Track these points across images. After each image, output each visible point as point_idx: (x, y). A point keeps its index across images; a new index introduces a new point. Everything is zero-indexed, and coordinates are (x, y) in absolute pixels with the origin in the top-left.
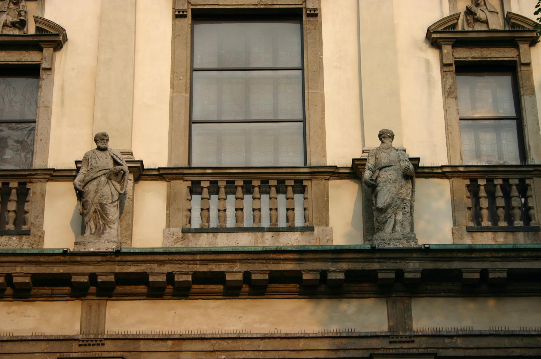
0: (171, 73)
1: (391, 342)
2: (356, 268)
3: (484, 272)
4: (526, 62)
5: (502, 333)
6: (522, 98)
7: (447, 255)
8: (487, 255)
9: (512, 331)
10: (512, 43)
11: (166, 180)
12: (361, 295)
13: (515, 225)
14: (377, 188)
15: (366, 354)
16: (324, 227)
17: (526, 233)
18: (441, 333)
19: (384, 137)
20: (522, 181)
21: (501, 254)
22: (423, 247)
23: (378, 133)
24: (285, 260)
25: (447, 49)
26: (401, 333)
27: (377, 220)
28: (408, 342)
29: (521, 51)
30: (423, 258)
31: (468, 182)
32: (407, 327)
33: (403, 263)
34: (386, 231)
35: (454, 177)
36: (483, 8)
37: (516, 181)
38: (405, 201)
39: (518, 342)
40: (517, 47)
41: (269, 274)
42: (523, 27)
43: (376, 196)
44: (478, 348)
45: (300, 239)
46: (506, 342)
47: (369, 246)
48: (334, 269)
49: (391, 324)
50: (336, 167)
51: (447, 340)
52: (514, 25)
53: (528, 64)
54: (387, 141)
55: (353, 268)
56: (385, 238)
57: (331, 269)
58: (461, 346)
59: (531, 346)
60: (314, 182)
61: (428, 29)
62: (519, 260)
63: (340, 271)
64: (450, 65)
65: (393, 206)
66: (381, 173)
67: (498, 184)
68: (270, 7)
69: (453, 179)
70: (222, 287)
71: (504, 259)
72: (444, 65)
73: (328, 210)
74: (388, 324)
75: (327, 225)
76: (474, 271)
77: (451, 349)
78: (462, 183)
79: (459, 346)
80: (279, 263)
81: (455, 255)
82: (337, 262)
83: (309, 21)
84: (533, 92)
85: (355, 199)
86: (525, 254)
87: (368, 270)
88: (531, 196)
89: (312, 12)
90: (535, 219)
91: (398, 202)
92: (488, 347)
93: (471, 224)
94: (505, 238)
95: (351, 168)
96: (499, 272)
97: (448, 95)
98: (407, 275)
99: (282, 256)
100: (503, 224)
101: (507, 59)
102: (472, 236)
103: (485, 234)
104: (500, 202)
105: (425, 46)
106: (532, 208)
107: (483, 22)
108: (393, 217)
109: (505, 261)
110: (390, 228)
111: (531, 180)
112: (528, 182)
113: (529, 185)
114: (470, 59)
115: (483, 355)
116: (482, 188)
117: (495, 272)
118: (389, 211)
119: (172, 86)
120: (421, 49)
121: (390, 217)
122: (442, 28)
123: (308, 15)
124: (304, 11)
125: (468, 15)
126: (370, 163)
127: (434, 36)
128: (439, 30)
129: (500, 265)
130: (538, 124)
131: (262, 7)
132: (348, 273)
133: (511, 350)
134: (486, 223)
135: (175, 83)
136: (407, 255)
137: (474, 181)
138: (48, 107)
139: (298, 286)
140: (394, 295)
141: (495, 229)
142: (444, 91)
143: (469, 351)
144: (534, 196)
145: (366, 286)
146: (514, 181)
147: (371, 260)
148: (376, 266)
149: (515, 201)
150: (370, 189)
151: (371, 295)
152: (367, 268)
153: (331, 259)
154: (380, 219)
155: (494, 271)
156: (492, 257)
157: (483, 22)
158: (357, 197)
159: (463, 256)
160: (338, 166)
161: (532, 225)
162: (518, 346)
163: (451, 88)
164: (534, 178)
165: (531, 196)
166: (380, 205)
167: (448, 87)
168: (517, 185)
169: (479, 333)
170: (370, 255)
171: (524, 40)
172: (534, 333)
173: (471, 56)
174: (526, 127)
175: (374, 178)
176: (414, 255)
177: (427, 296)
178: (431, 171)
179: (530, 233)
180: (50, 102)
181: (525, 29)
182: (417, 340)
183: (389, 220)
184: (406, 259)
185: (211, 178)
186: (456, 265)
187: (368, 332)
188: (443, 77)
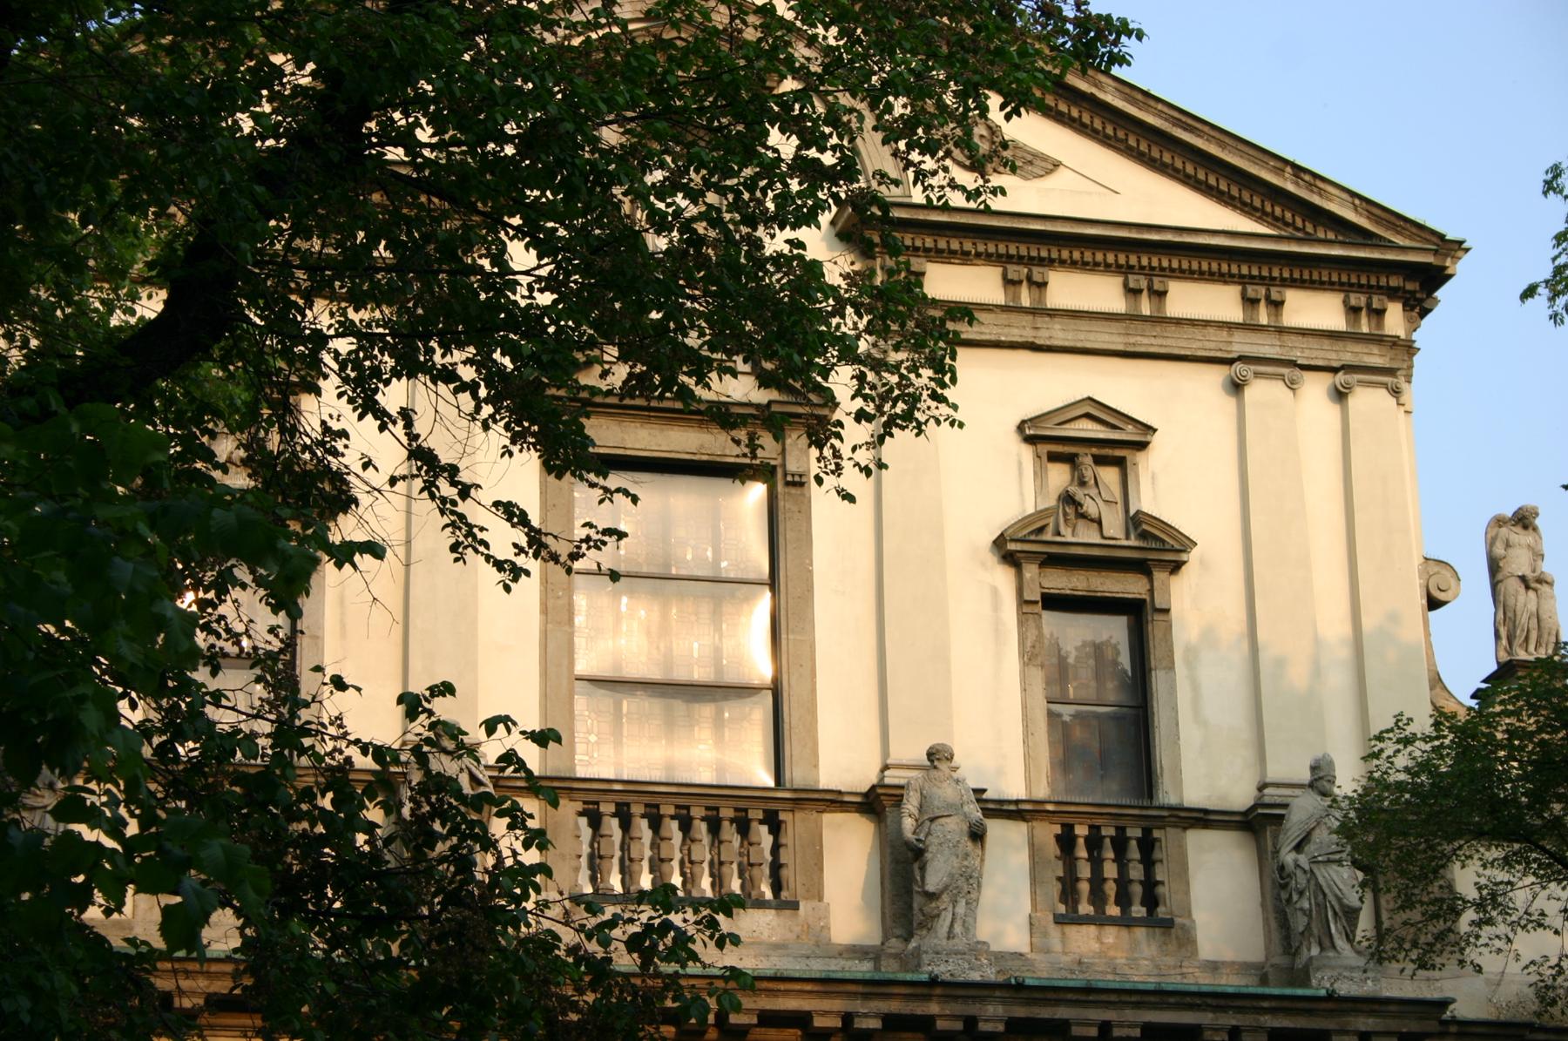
0: (541, 583)
2: (903, 1012)
3: (1105, 1027)
7: (1051, 995)
8: (1113, 998)
10: (1142, 567)
11: (537, 797)
13: (1134, 915)
16: (815, 903)
17: (1151, 930)
20: (1147, 832)
21: (1134, 999)
22: (1013, 981)
24: (787, 992)
25: (1031, 571)
29: (1156, 584)
31: (1058, 829)
33: (978, 1006)
34: (940, 935)
36: (1093, 492)
38: (971, 881)
40: (1148, 574)
41: (759, 1016)
42: (1163, 541)
43: (923, 869)
45: (774, 923)
47: (927, 976)
50: (840, 792)
52: (1144, 535)
53: (1167, 611)
54: (943, 766)
55: (896, 1011)
56: (939, 948)
60: (799, 815)
61: (1002, 534)
62: (1161, 1009)
63: (876, 1016)
64: (1035, 602)
66: (933, 826)
68: (718, 459)
70: (673, 1029)
71: (1137, 1005)
72: (1022, 602)
73: (821, 870)
75: (821, 899)
78: (1048, 832)
80: (776, 996)
81: (1062, 996)
83: (789, 494)
84: (1171, 667)
85: (870, 854)
86: (1172, 1000)
87: (921, 1016)
89: (797, 479)
90: (1165, 905)
91: (959, 883)
93: (1062, 909)
94: (1117, 937)
95: (866, 795)
96: (1129, 1026)
98: (984, 1027)
99: (782, 986)
100: (1113, 910)
102: (1063, 934)
103: (1084, 928)
104: (1110, 870)
105: (992, 559)
106: (1162, 883)
107: (1092, 520)
108: (950, 909)
109: (1139, 1008)
110: (945, 929)
112: (1156, 834)
113: (1159, 840)
114: (1068, 592)
116: (1081, 841)
117: (1122, 1026)
118: (945, 897)
119: (545, 610)
120: (983, 564)
122: (1026, 532)
123: (788, 484)
124: (779, 472)
125: (1068, 503)
126: (911, 804)
127: (1012, 546)
128: (1020, 535)
129: (1130, 1015)
130: (1177, 724)
131: (705, 458)
134: (1085, 908)
135: (550, 604)
136: (986, 993)
137: (1068, 829)
138: (318, 637)
139: (799, 1033)
141: (1100, 920)
142: (1022, 653)
146: (1134, 832)
147: (927, 998)
148: (934, 1008)
149: (1134, 868)
150: (910, 854)
152: (919, 1012)
153: (862, 994)
154: (926, 909)
155: (1121, 1025)
156: (1120, 1002)
157: (1092, 520)
158: (872, 848)
160: (843, 790)
161: (1160, 916)
163: (1034, 647)
164: (1168, 829)
165: (1161, 861)
166: (931, 887)
167: (1029, 644)
170: (925, 991)
171: (1162, 564)
173: (1070, 586)
175: (922, 837)
176: (998, 993)
178: (998, 807)
179: (1157, 930)
180: (321, 627)
181: (1167, 547)
185: (619, 798)
186: (1062, 1013)
188: (1021, 623)
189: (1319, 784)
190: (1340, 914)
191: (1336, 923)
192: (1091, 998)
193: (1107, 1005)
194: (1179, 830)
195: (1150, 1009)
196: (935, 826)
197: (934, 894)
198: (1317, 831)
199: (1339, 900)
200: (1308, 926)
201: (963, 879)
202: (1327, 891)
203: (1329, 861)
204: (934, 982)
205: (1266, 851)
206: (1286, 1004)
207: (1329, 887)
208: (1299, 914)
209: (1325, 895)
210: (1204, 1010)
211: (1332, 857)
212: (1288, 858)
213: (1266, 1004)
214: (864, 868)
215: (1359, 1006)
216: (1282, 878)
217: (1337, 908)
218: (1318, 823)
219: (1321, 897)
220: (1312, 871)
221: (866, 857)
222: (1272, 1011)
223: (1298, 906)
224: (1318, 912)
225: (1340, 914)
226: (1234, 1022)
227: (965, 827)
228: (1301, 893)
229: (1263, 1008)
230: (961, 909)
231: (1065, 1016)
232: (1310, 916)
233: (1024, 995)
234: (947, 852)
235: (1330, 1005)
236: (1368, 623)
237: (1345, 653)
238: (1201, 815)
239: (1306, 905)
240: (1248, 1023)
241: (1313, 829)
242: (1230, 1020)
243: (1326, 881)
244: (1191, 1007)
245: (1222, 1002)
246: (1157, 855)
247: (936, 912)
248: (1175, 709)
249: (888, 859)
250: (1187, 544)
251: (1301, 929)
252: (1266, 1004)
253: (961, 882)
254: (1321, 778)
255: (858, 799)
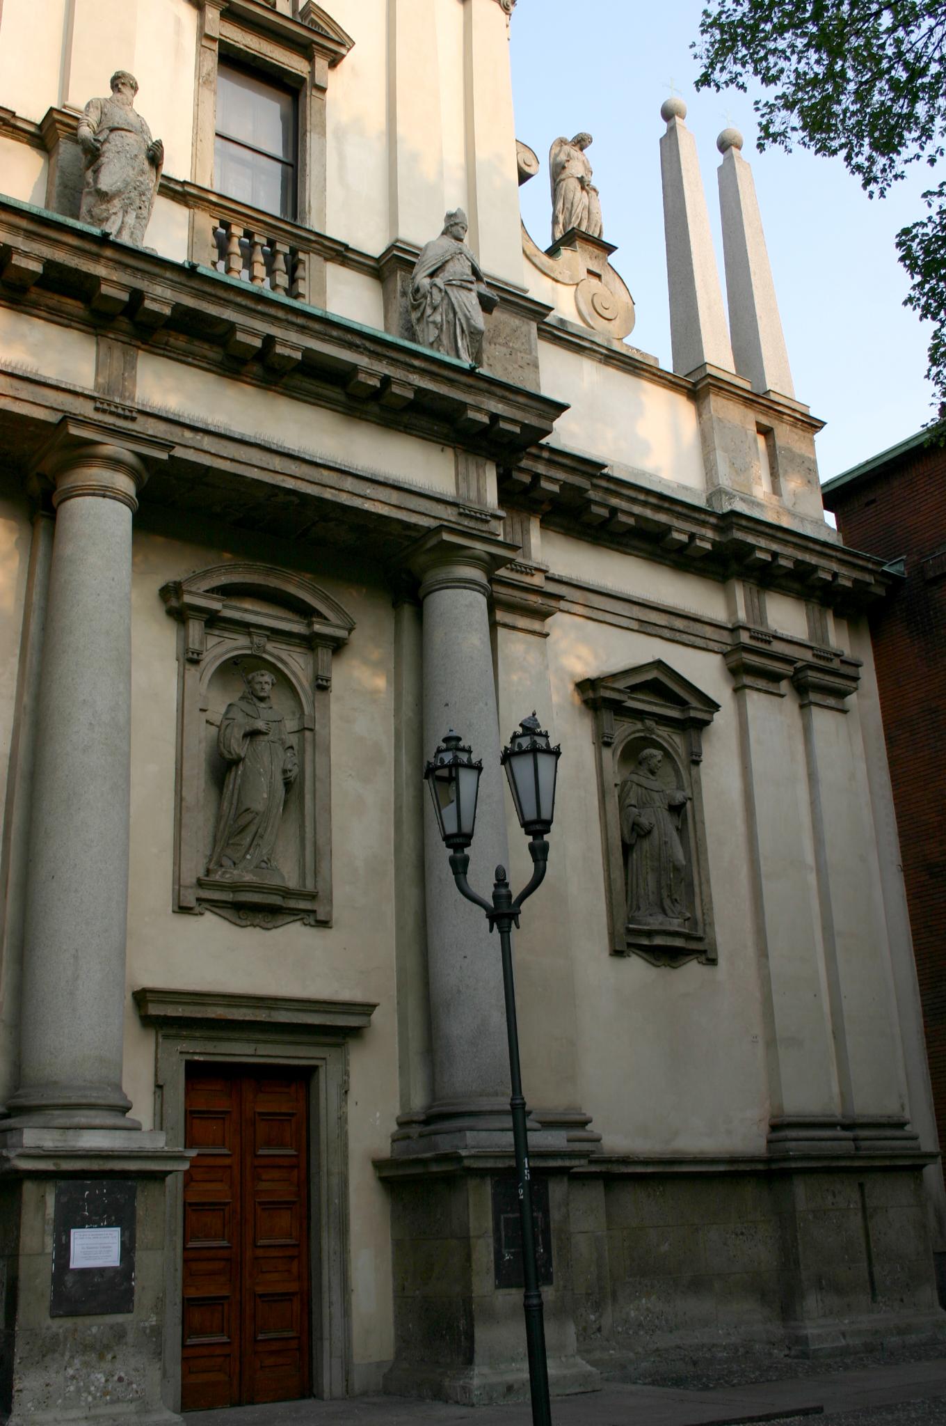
1: (97, 409)
2: (66, 263)
3: (269, 340)
4: (322, 85)
5: (274, 447)
6: (308, 134)
8: (281, 314)
9: (289, 449)
10: (306, 50)
12: (57, 317)
14: (102, 158)
15: (53, 418)
18: (182, 420)
19: (123, 84)
20: (294, 252)
23: (112, 75)
26: (117, 400)
27: (90, 211)
28: (126, 418)
29: (316, 66)
30: (180, 284)
32: (127, 394)
33: (146, 283)
35: (199, 207)
37: (286, 250)
38: (144, 198)
39: (293, 467)
42: (328, 33)
44: (232, 460)
46: (277, 463)
48: (26, 250)
49: (101, 380)
50: (13, 114)
51: (188, 434)
53: (323, 90)
55: (61, 261)
57: (22, 248)
58: (209, 450)
59: (311, 479)
62: (323, 340)
63: (38, 258)
65: (123, 196)
67: (259, 244)
69: (196, 210)
71: (302, 329)
74: (96, 379)
76: (253, 333)
77: (192, 450)
78: (208, 222)
79: (206, 448)
82: (33, 240)
84: (323, 134)
86: (335, 333)
88: (304, 279)
92: (249, 462)
95: (40, 127)
97: (204, 83)
98: (148, 304)
101: (294, 71)
108: (120, 214)
109: (303, 333)
111: (307, 256)
112: (301, 256)
113: (303, 262)
114: (242, 47)
115: (239, 472)
117: (285, 346)
118: (116, 202)
121: (115, 214)
129: (293, 337)
130: (325, 180)
132: (49, 264)
133: (281, 477)
136: (157, 270)
140: (112, 336)
142: (198, 76)
143: (220, 461)
144: (307, 279)
145: (72, 305)
147: (96, 257)
148: (100, 270)
149: (280, 276)
151: (73, 324)
153: (26, 230)
154: (96, 211)
155: (285, 343)
159: (244, 303)
162: (292, 474)
164: (311, 254)
165: (304, 279)
168: (285, 255)
169: (239, 437)
170: (93, 248)
172: (319, 461)
173: (244, 42)
174: (308, 178)
176: (168, 275)
177: (163, 356)
182: (141, 419)
183: (113, 217)
184: (153, 277)
187: (62, 381)
188: (199, 54)
189: (454, 229)
190: (466, 332)
191: (462, 339)
192: (259, 308)
193: (274, 320)
194: (321, 259)
195: (312, 336)
196: (114, 135)
197: (106, 194)
198: (451, 264)
199: (468, 319)
200: (438, 338)
201: (136, 193)
202: (458, 309)
203: (461, 287)
204: (104, 240)
205: (395, 291)
206: (434, 368)
207: (460, 306)
208: (431, 326)
209: (455, 313)
210: (362, 353)
211: (465, 284)
212: (426, 282)
213: (416, 363)
214: (31, 193)
215: (494, 389)
216: (415, 300)
217: (465, 326)
218: (452, 258)
219: (451, 315)
220: (446, 292)
221: (33, 185)
222: (422, 372)
223: (431, 319)
224: (448, 329)
225: (466, 332)
226: (387, 372)
227: (144, 148)
228: (435, 309)
229: (414, 367)
230: (131, 219)
231: (232, 319)
232: (441, 330)
233: (195, 284)
234: (123, 159)
235: (470, 381)
236: (481, 154)
237: (460, 175)
238: (342, 249)
239: (438, 318)
240: (398, 377)
241: (447, 262)
242: (384, 369)
243: (458, 302)
244: (351, 346)
245: (379, 349)
246: (300, 273)
247: (105, 214)
248: (324, 166)
249: (57, 181)
250: (345, 42)
251: (432, 339)
252: (416, 363)
253: (134, 194)
254: (456, 224)
255: (32, 129)
